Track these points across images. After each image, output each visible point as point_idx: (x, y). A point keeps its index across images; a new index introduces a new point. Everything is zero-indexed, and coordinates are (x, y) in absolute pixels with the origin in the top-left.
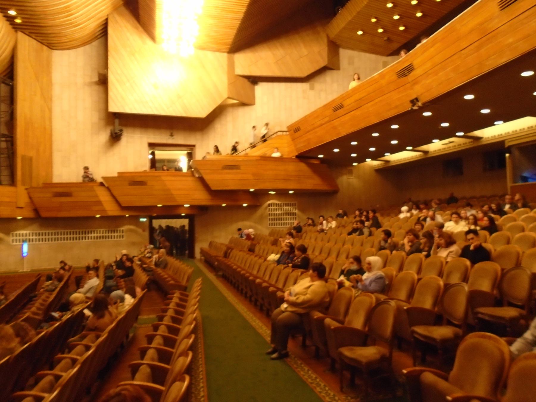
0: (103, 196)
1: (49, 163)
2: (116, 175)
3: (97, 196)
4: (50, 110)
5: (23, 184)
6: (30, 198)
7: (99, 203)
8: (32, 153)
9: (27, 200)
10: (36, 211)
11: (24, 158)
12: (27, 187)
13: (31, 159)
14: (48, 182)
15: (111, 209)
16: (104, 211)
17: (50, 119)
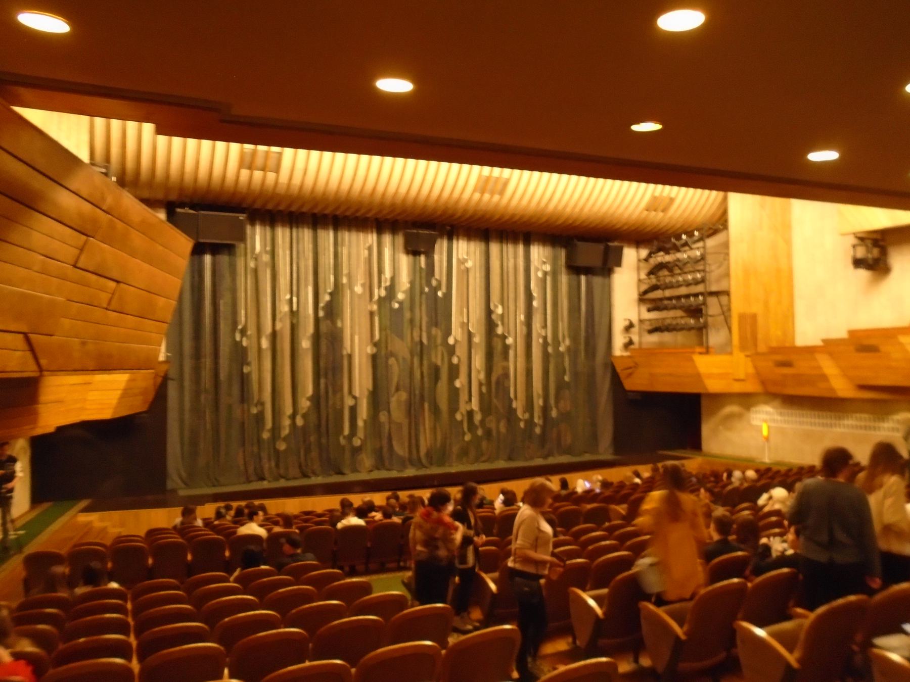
0: (829, 367)
1: (789, 317)
2: (843, 334)
3: (820, 368)
4: (788, 242)
5: (743, 348)
6: (756, 368)
7: (824, 378)
8: (756, 308)
9: (751, 370)
10: (763, 383)
11: (742, 317)
12: (748, 353)
13: (754, 317)
14: (787, 345)
15: (842, 387)
16: (832, 390)
17: (789, 256)
